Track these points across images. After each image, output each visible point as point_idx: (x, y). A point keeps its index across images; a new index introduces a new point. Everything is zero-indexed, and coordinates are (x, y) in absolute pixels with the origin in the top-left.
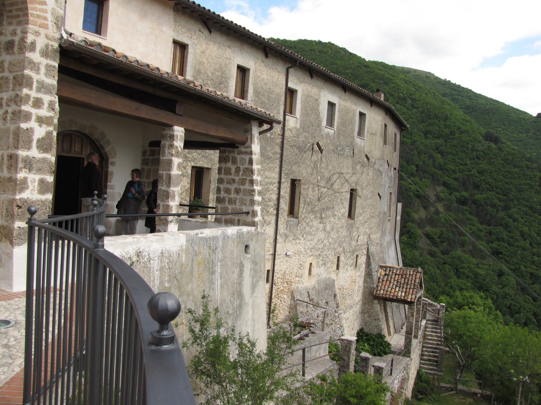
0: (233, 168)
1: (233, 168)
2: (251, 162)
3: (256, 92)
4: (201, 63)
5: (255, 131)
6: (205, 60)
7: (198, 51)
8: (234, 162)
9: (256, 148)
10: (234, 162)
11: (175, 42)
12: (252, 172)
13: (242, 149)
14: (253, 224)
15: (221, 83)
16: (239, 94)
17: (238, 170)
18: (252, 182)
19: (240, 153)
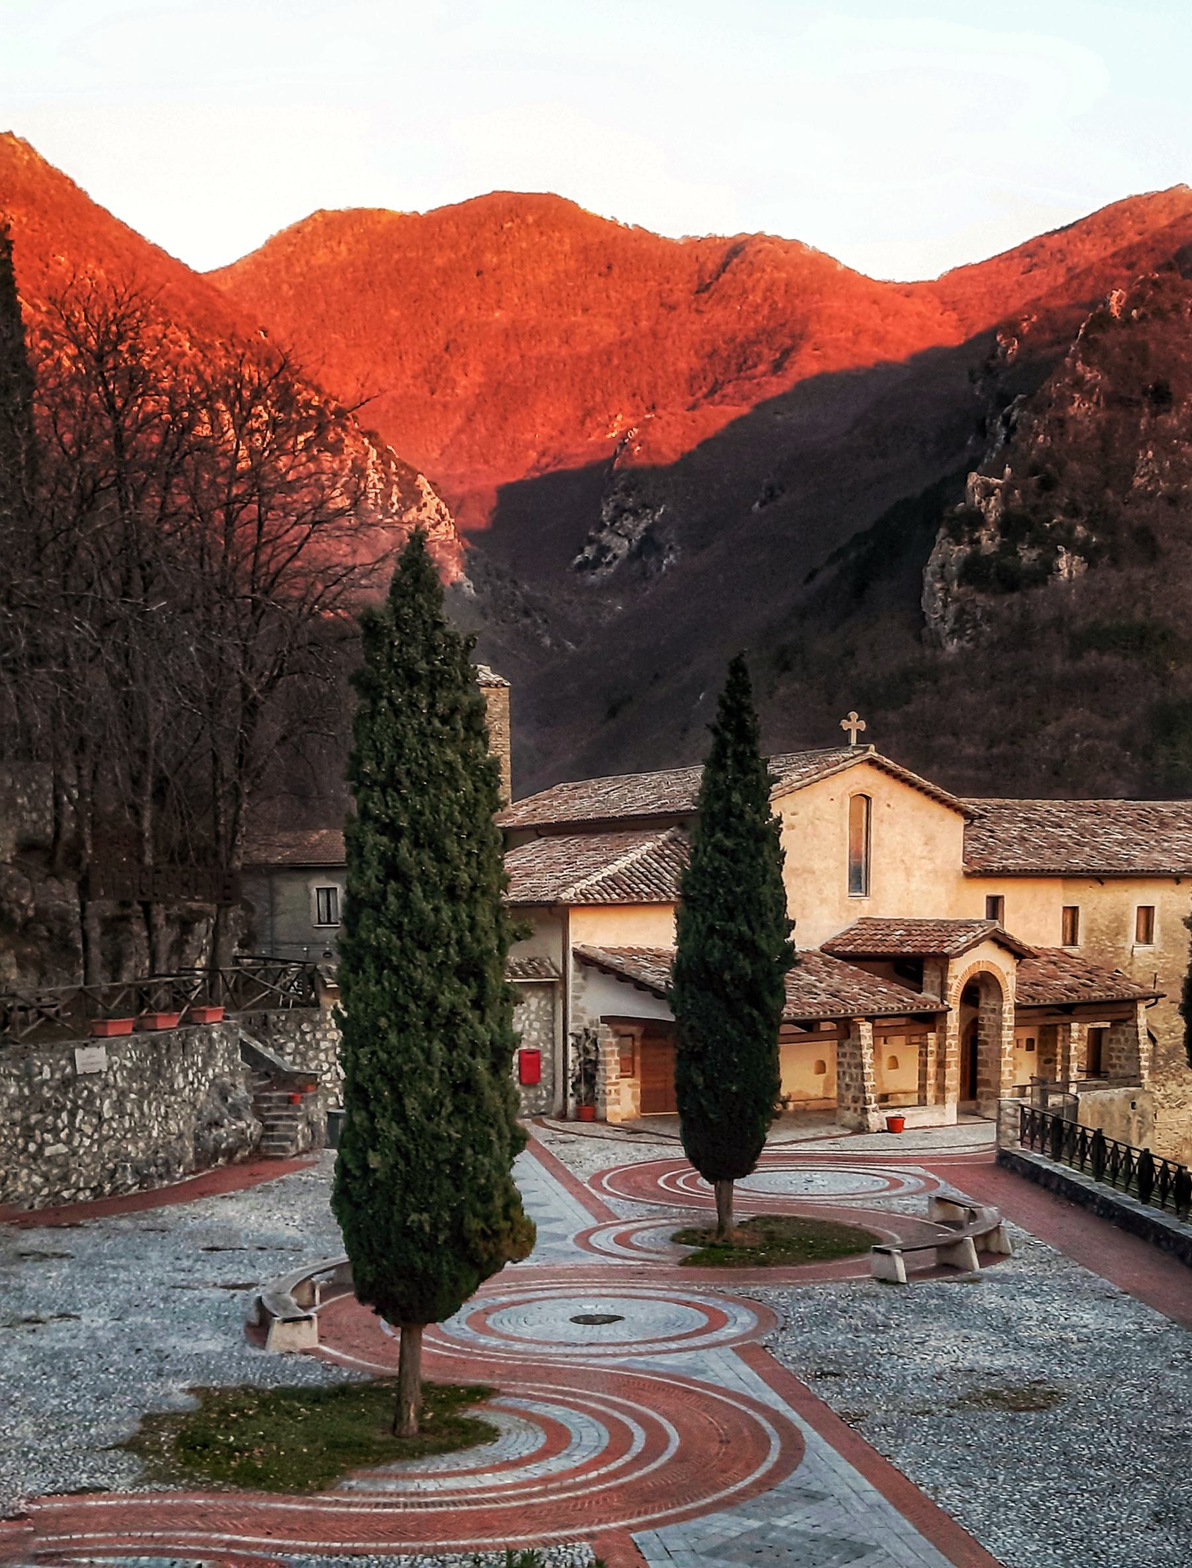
0: (1122, 1039)
1: (1122, 1039)
2: (1137, 1034)
3: (1162, 930)
4: (1094, 921)
5: (1141, 1007)
6: (1097, 916)
7: (1090, 909)
8: (1124, 1033)
9: (1142, 1021)
10: (1124, 1033)
11: (1065, 908)
12: (1138, 1042)
13: (1130, 1023)
14: (1140, 1085)
15: (1117, 934)
16: (1142, 935)
17: (1127, 1040)
18: (1138, 1050)
19: (1128, 1026)
